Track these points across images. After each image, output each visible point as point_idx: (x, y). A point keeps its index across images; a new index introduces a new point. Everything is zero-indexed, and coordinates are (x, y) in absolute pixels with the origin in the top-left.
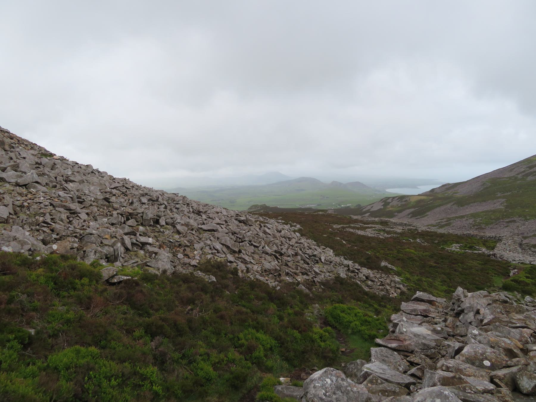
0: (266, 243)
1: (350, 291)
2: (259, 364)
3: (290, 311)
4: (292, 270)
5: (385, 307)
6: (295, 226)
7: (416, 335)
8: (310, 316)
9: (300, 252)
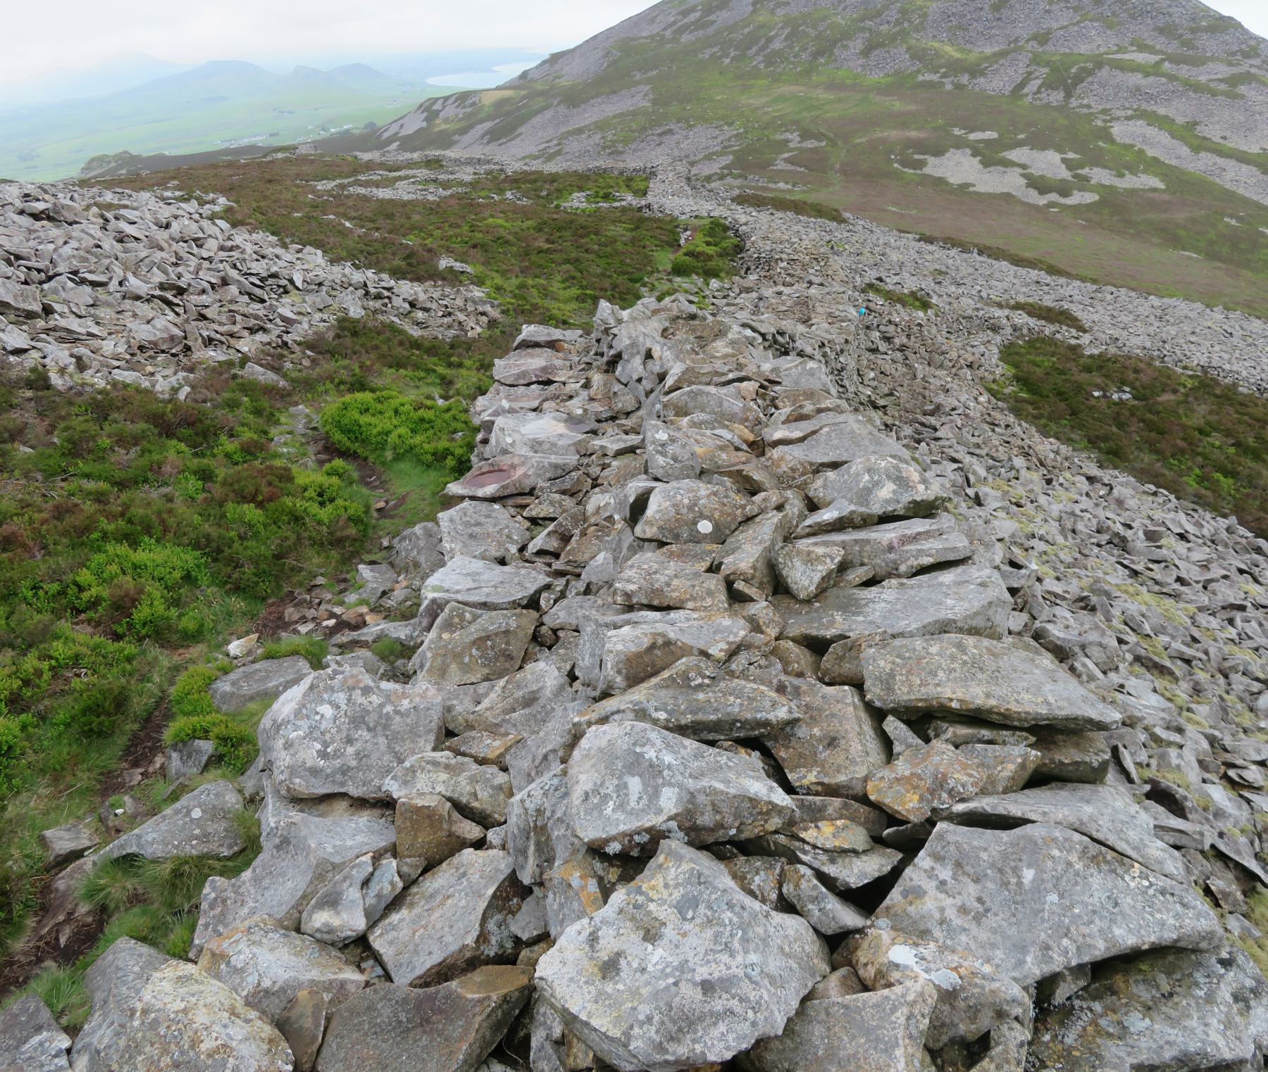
0: (126, 269)
1: (376, 347)
2: (161, 634)
3: (231, 446)
4: (220, 329)
5: (460, 365)
6: (213, 202)
7: (536, 445)
8: (285, 444)
9: (234, 274)
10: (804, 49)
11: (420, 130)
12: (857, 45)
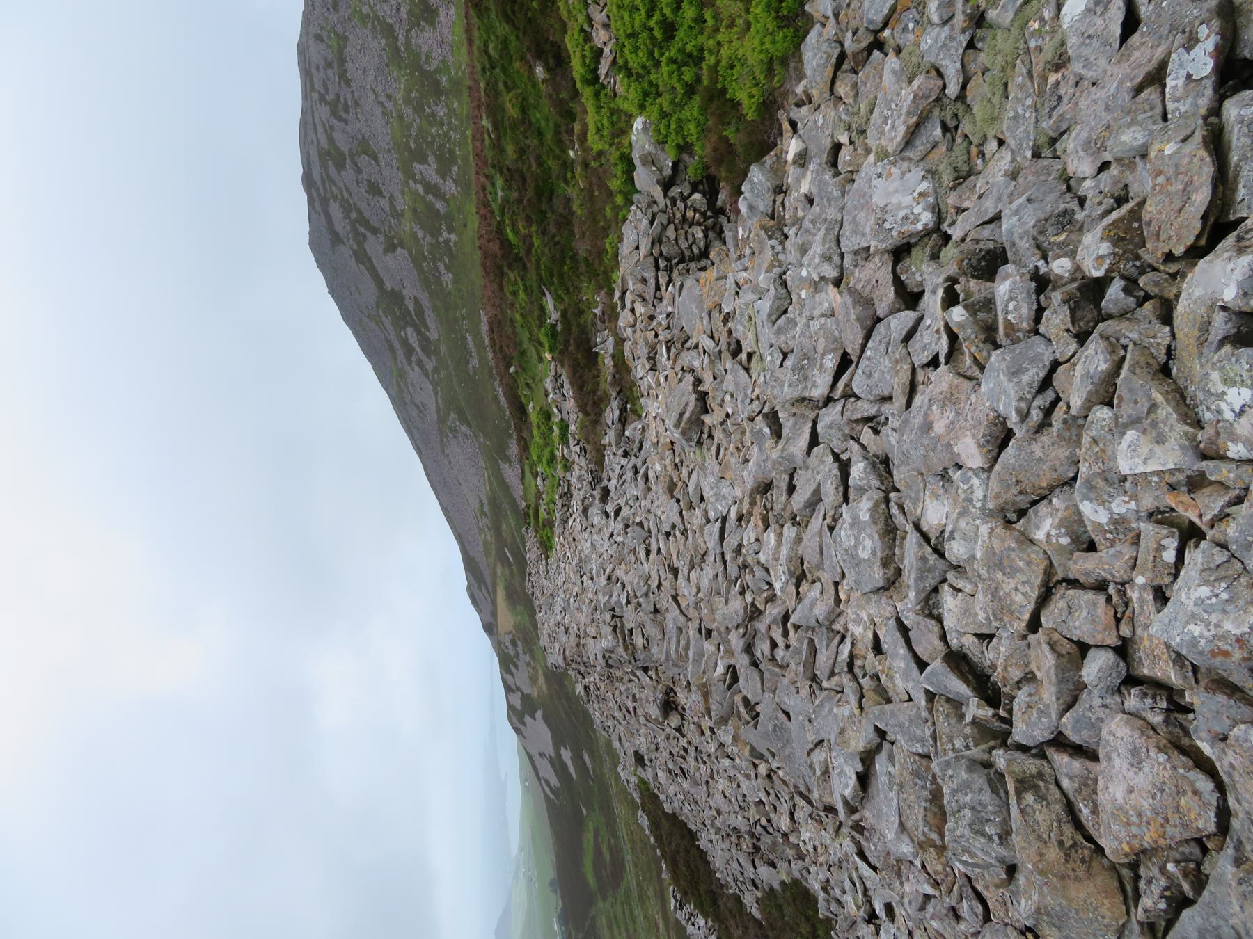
10: (432, 119)
11: (546, 719)
12: (425, 40)
